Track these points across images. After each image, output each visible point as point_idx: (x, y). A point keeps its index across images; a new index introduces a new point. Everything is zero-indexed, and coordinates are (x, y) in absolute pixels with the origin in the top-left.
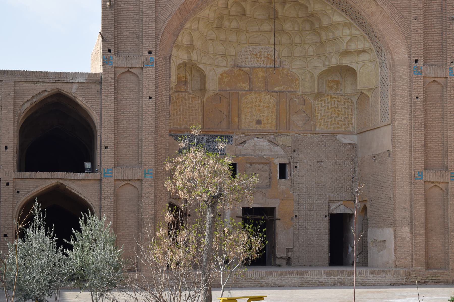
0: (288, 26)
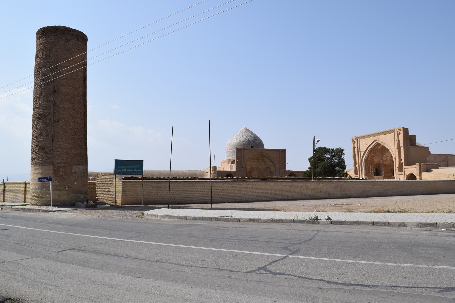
0: (260, 161)
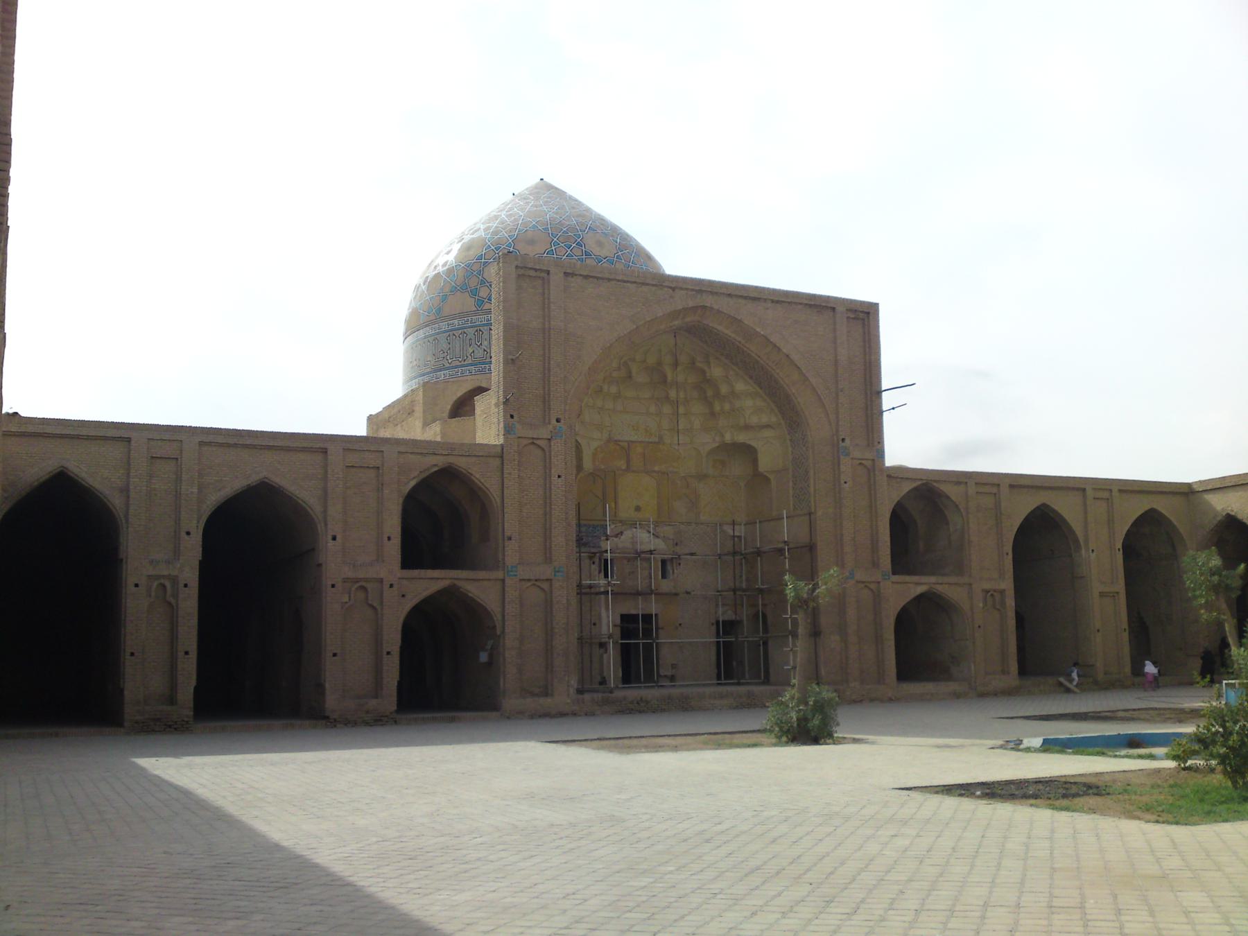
0: (673, 394)
